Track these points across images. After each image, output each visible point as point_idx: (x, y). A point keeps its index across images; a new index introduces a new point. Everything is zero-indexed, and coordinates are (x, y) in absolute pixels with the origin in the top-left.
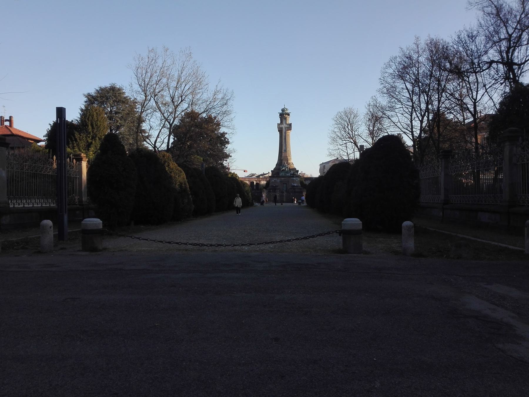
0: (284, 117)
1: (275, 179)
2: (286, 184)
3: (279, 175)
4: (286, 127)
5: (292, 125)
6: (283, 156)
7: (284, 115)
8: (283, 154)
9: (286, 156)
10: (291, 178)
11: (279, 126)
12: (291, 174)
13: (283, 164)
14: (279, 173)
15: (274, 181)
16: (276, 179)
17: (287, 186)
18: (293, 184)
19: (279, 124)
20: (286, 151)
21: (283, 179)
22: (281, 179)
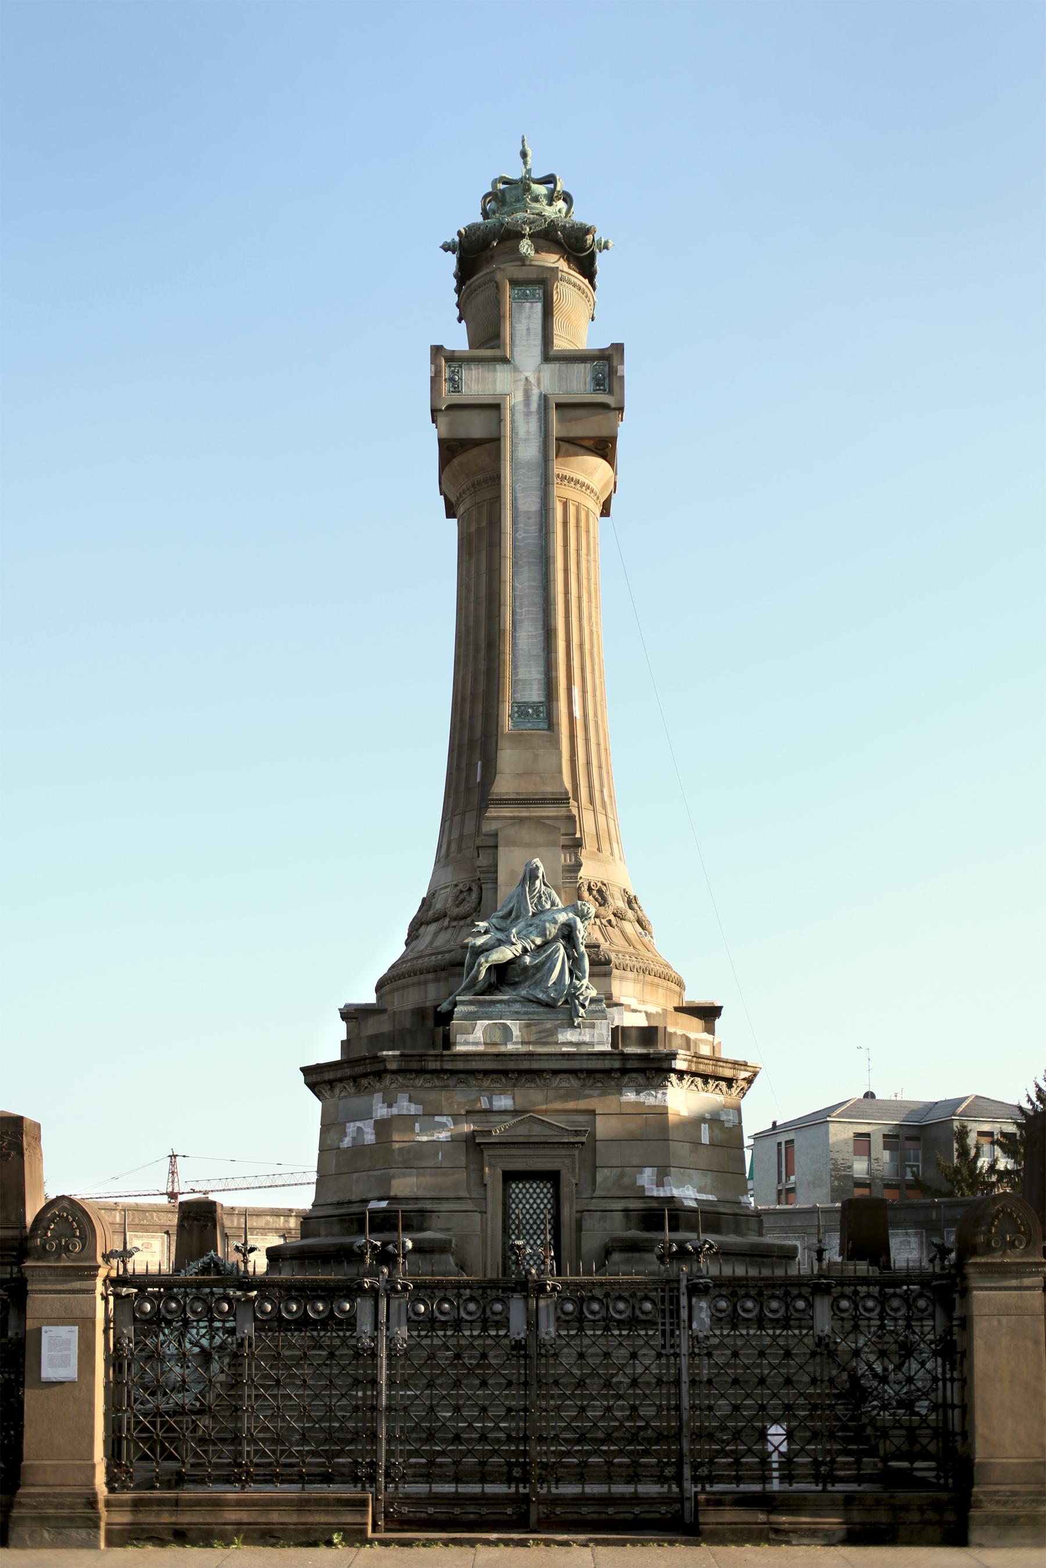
0: (523, 260)
1: (381, 1111)
2: (553, 1177)
3: (448, 1043)
4: (545, 399)
5: (630, 369)
6: (504, 785)
7: (526, 247)
8: (508, 758)
9: (549, 789)
10: (630, 1096)
11: (456, 388)
12: (619, 1034)
13: (506, 889)
14: (449, 1015)
15: (370, 1137)
16: (405, 1106)
17: (567, 1213)
18: (646, 1178)
19: (452, 358)
20: (551, 725)
21: (504, 1102)
22: (484, 1104)
